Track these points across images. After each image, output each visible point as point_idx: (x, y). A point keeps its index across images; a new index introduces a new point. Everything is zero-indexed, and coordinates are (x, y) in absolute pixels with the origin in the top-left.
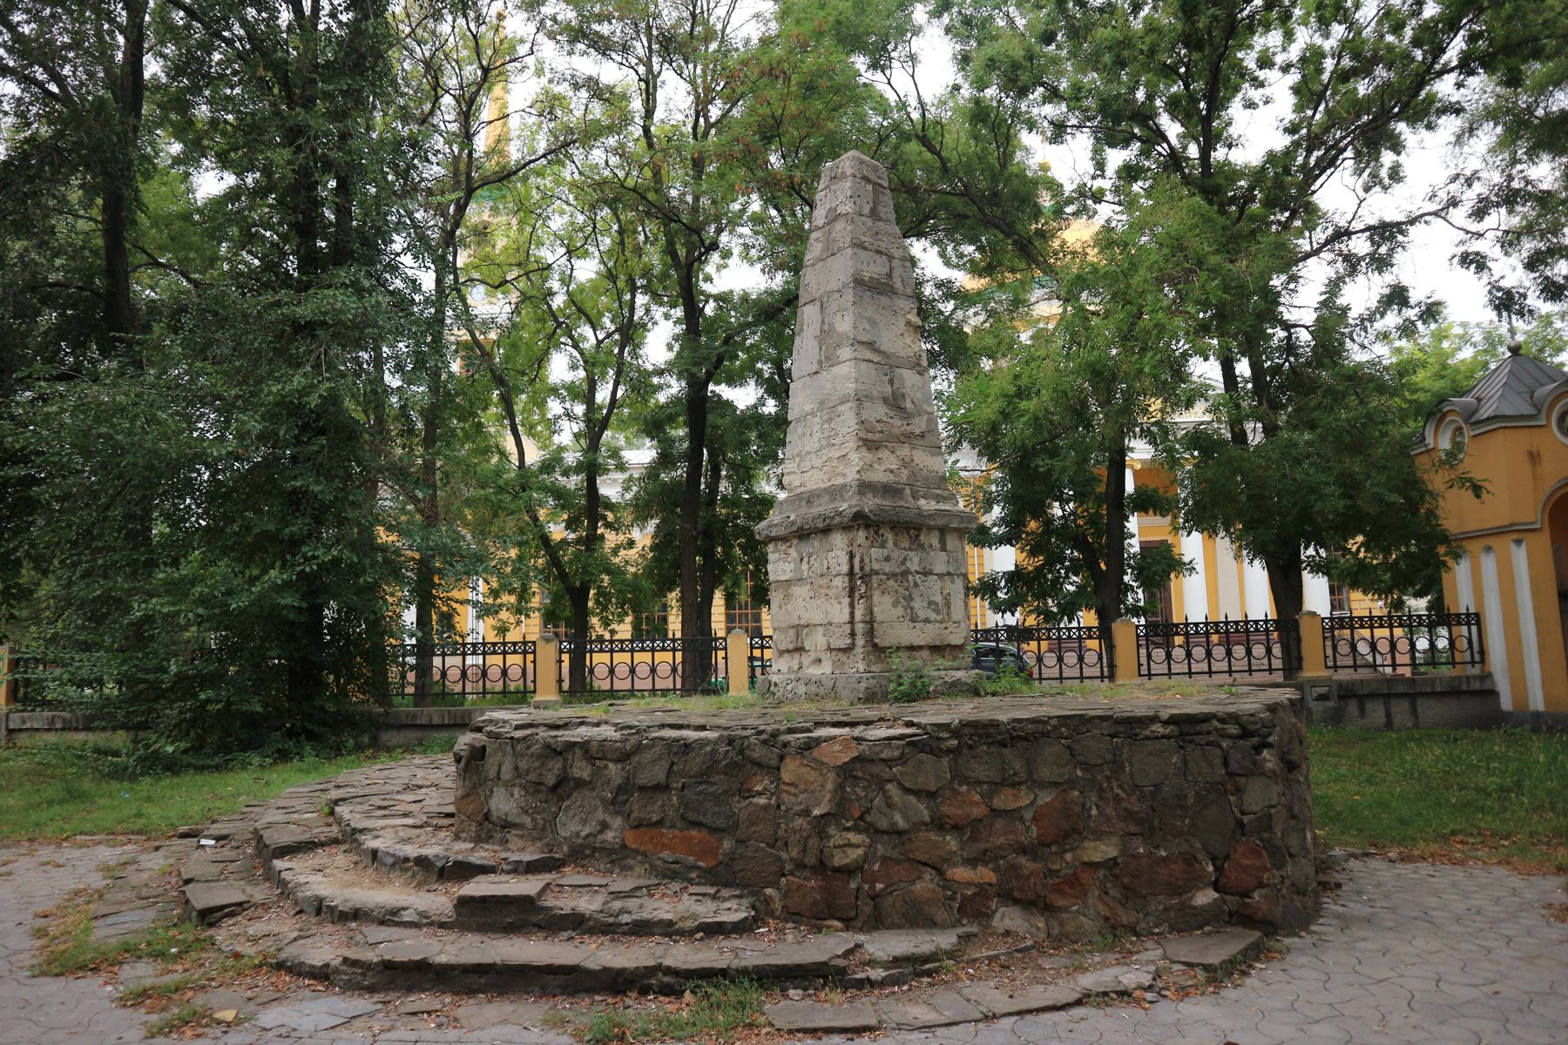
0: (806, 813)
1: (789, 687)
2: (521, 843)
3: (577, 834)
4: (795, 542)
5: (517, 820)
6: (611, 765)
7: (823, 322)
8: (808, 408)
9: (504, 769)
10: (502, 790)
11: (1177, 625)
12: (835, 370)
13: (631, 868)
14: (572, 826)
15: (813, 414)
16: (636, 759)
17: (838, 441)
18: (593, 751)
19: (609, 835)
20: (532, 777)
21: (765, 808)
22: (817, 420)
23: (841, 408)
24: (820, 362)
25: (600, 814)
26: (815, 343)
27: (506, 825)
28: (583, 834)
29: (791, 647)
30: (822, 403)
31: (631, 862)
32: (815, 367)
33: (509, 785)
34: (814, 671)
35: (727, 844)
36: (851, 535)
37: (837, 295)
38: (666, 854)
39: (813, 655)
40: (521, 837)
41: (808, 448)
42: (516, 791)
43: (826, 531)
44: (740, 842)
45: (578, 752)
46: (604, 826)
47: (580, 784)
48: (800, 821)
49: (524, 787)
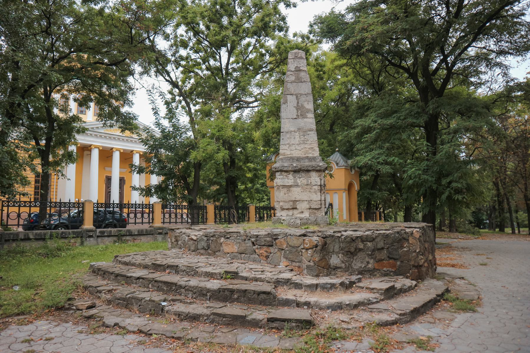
0: (415, 251)
1: (292, 221)
2: (342, 274)
3: (361, 267)
5: (340, 266)
6: (368, 243)
7: (298, 103)
8: (292, 129)
9: (335, 248)
10: (335, 255)
11: (125, 204)
12: (305, 119)
13: (376, 275)
14: (357, 264)
15: (294, 131)
16: (376, 240)
17: (309, 142)
18: (364, 239)
19: (370, 266)
20: (346, 249)
21: (407, 251)
22: (297, 134)
23: (309, 132)
24: (297, 115)
25: (367, 259)
26: (295, 109)
27: (336, 268)
28: (363, 267)
29: (291, 207)
31: (376, 273)
32: (295, 117)
33: (337, 253)
34: (302, 216)
35: (398, 263)
36: (320, 173)
37: (304, 96)
38: (385, 269)
39: (300, 211)
40: (341, 271)
41: (293, 142)
42: (340, 255)
43: (308, 171)
44: (402, 262)
45: (359, 240)
46: (368, 263)
47: (360, 250)
48: (414, 254)
49: (343, 254)
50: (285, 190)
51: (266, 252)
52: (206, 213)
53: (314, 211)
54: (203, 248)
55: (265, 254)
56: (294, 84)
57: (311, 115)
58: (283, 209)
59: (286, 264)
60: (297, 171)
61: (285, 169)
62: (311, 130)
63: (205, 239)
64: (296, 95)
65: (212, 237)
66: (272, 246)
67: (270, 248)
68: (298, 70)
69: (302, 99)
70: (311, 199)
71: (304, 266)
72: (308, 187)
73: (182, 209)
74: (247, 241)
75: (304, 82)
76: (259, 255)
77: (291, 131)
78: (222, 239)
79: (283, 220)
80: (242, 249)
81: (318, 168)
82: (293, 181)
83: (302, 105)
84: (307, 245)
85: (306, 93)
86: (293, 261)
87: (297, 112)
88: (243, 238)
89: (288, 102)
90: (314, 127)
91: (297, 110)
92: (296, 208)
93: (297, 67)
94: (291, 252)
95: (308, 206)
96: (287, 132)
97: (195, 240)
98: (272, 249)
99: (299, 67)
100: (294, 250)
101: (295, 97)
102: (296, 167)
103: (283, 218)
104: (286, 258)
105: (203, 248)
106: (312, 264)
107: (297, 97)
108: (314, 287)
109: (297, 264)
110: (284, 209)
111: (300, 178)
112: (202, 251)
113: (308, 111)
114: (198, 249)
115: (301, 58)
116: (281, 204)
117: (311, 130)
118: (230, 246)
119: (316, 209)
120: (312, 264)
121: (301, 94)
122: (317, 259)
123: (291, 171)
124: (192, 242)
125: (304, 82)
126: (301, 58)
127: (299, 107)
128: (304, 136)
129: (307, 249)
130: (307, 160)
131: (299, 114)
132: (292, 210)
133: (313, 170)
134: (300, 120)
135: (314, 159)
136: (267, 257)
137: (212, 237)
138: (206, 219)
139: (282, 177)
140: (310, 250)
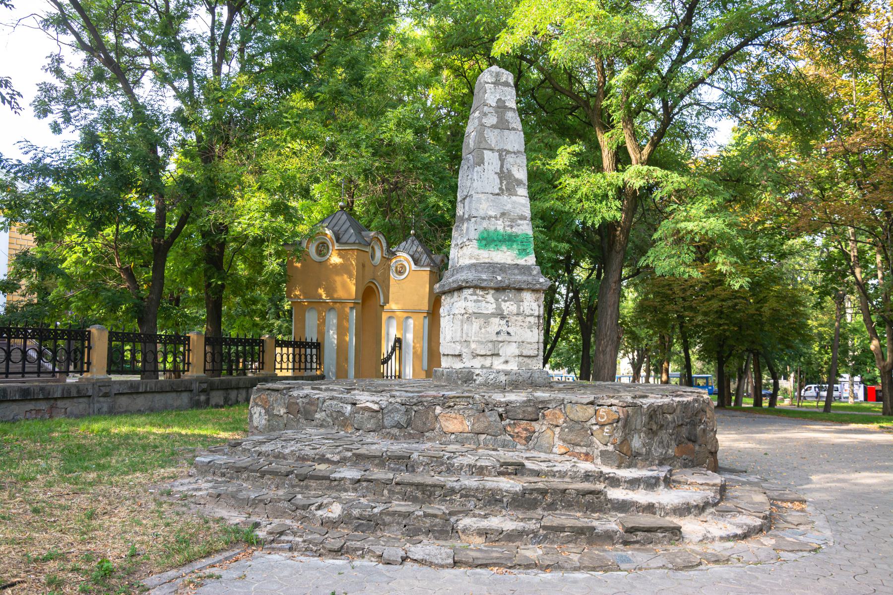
1: (492, 377)
4: (492, 292)
7: (502, 166)
8: (493, 214)
12: (514, 198)
15: (496, 217)
22: (500, 222)
23: (520, 222)
24: (501, 189)
26: (496, 176)
29: (489, 353)
30: (503, 214)
32: (497, 191)
36: (538, 295)
37: (513, 155)
43: (520, 290)
50: (482, 320)
51: (526, 430)
52: (90, 348)
53: (525, 359)
54: (398, 426)
55: (524, 434)
56: (497, 131)
57: (523, 191)
58: (475, 356)
59: (563, 450)
60: (500, 289)
61: (484, 284)
62: (523, 218)
63: (403, 408)
64: (500, 151)
65: (415, 404)
66: (536, 420)
67: (533, 423)
68: (501, 107)
69: (510, 159)
70: (523, 339)
71: (597, 452)
72: (520, 318)
73: (56, 340)
74: (487, 413)
75: (513, 129)
76: (512, 436)
77: (491, 217)
78: (438, 410)
79: (477, 375)
80: (479, 427)
81: (538, 286)
82: (494, 306)
83: (509, 171)
84: (602, 418)
85: (515, 150)
87: (501, 183)
88: (480, 407)
89: (486, 164)
91: (500, 178)
92: (498, 355)
93: (500, 100)
94: (571, 431)
95: (517, 352)
96: (484, 218)
98: (536, 426)
99: (504, 102)
100: (578, 427)
101: (497, 154)
102: (501, 281)
103: (477, 372)
104: (564, 441)
105: (398, 426)
106: (610, 448)
107: (500, 156)
108: (633, 483)
109: (584, 450)
110: (478, 355)
111: (505, 301)
112: (395, 431)
113: (519, 183)
114: (384, 427)
115: (506, 84)
116: (473, 346)
117: (523, 218)
118: (455, 421)
119: (529, 357)
120: (610, 448)
121: (508, 152)
122: (618, 442)
123: (492, 288)
125: (513, 129)
126: (506, 84)
127: (504, 175)
128: (512, 227)
129: (602, 425)
130: (516, 271)
131: (504, 187)
132: (490, 358)
133: (528, 289)
134: (505, 198)
137: (415, 404)
138: (89, 363)
139: (475, 297)
140: (607, 427)
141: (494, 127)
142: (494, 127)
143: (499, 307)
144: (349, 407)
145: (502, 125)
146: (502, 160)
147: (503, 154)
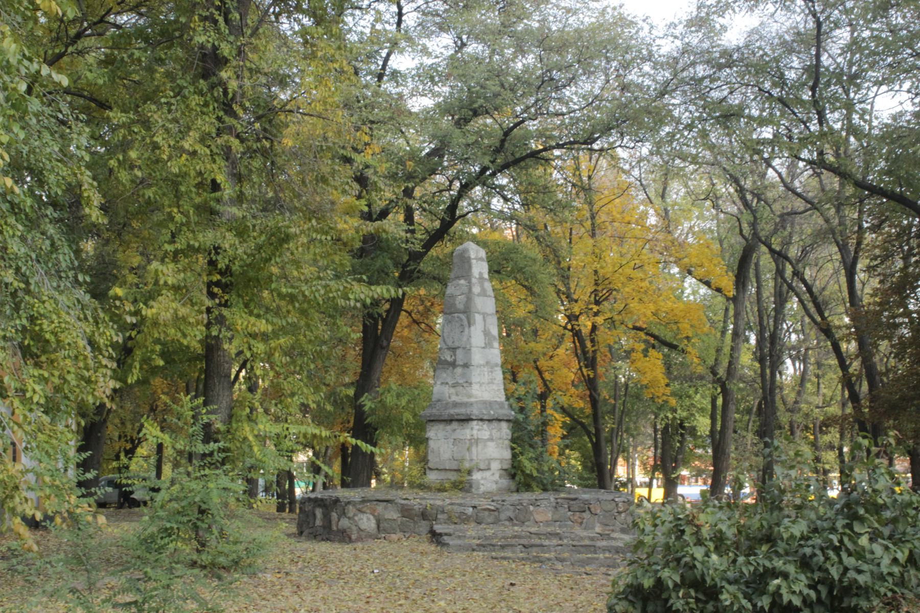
32: (483, 345)
55: (580, 520)
56: (481, 298)
62: (496, 365)
63: (512, 508)
66: (584, 511)
71: (618, 529)
78: (531, 508)
80: (556, 517)
86: (607, 525)
90: (499, 360)
97: (493, 511)
98: (584, 515)
100: (607, 514)
109: (611, 528)
112: (507, 523)
113: (494, 337)
117: (496, 365)
121: (488, 315)
124: (487, 513)
126: (481, 259)
127: (486, 333)
135: (501, 405)
136: (581, 523)
141: (479, 295)
142: (479, 295)
143: (491, 435)
144: (471, 509)
145: (483, 293)
146: (485, 320)
147: (485, 315)
